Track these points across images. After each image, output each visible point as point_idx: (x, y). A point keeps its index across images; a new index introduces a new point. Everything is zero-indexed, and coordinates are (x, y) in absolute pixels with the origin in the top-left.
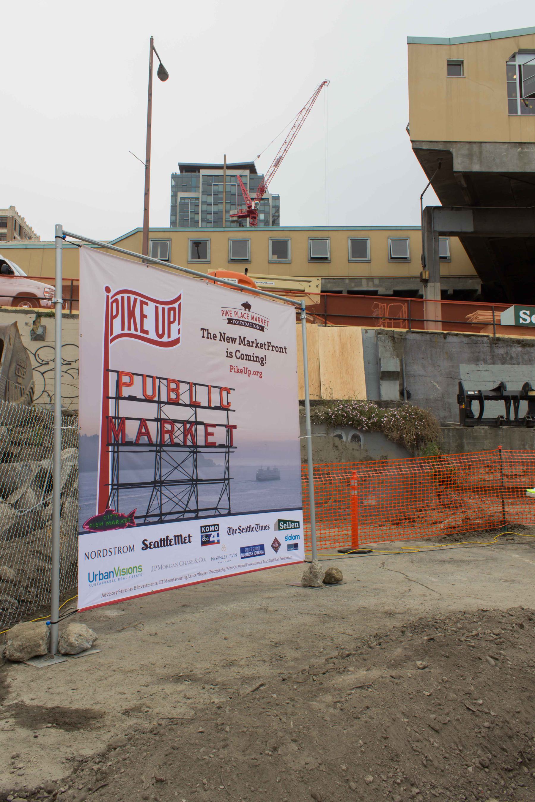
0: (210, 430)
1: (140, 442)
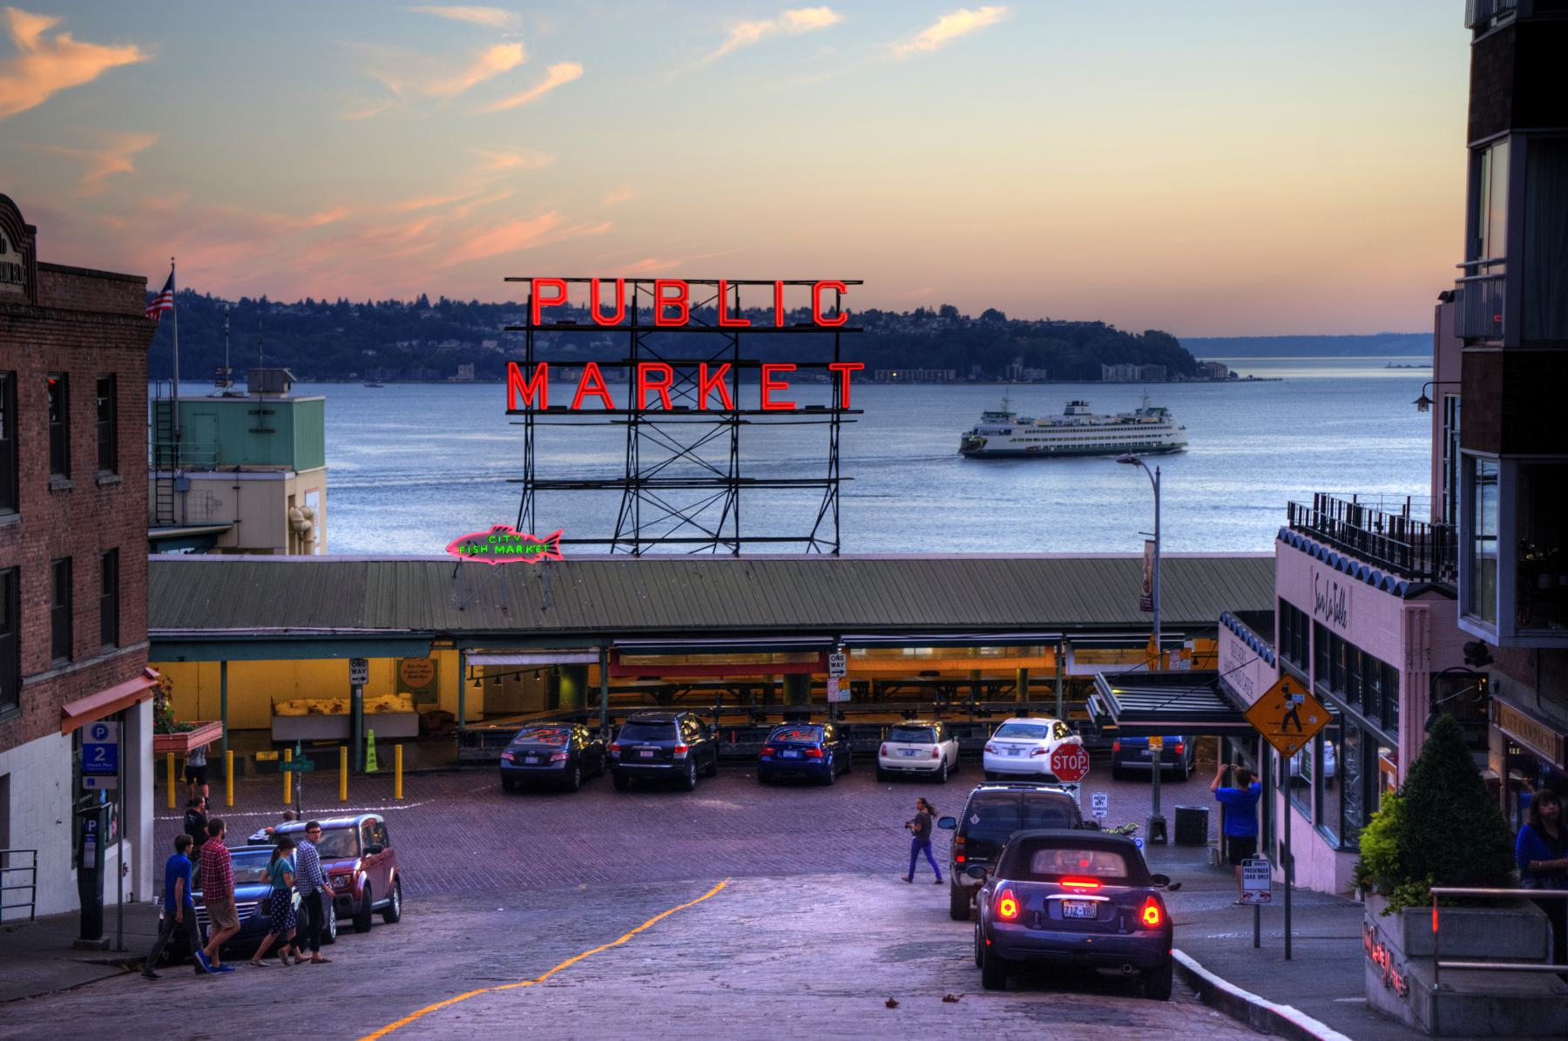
1: (584, 406)
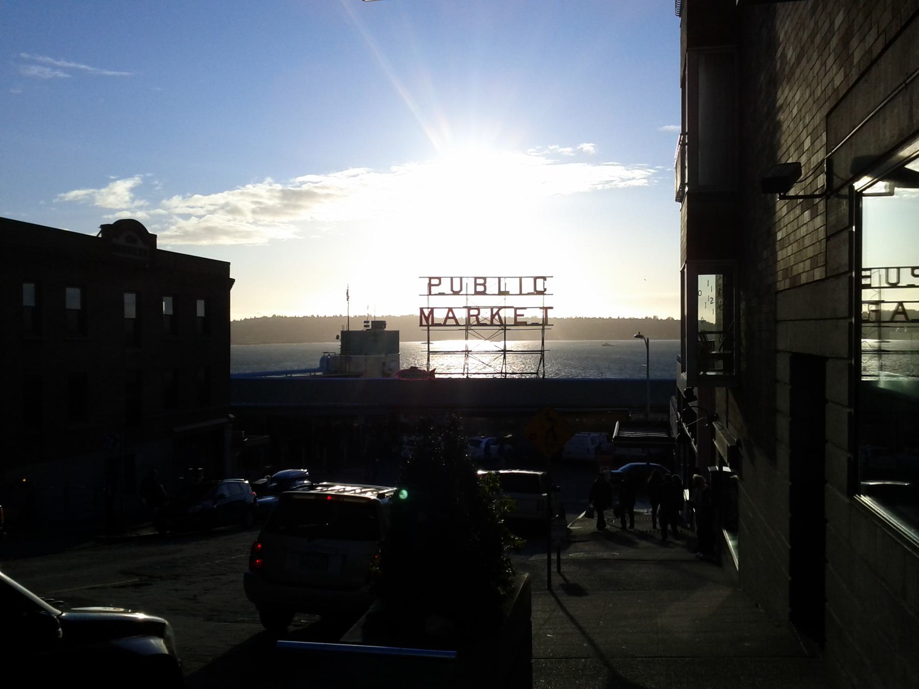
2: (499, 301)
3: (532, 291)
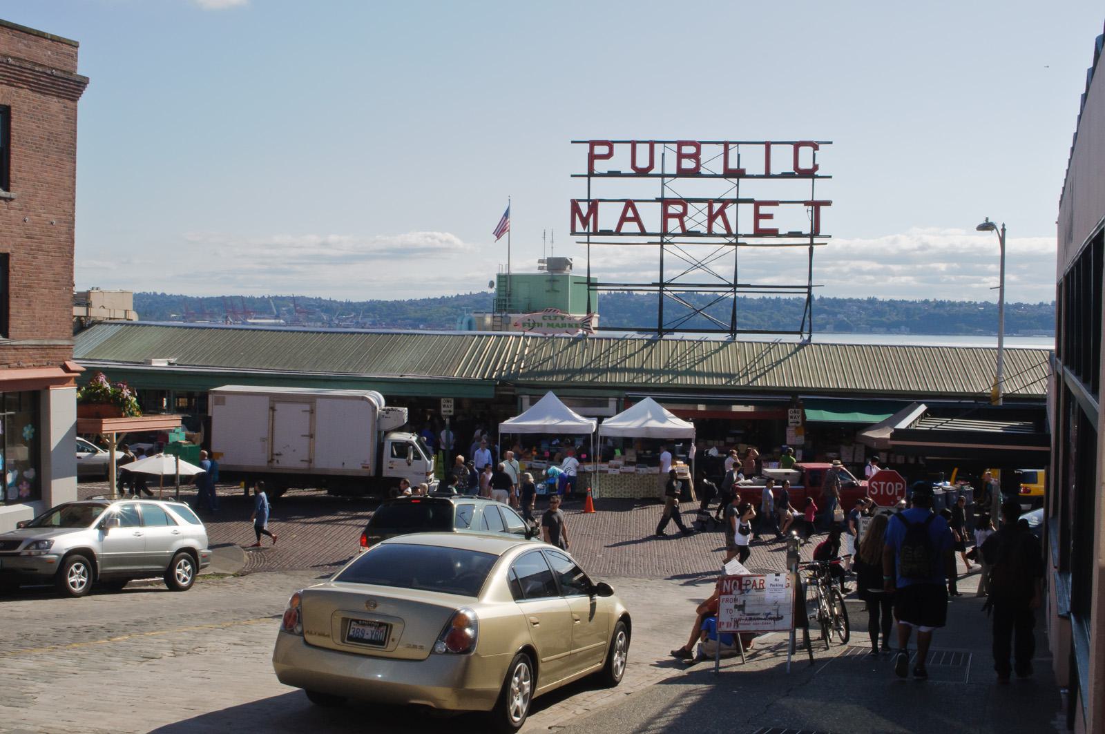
0: (763, 210)
2: (724, 188)
3: (791, 169)
